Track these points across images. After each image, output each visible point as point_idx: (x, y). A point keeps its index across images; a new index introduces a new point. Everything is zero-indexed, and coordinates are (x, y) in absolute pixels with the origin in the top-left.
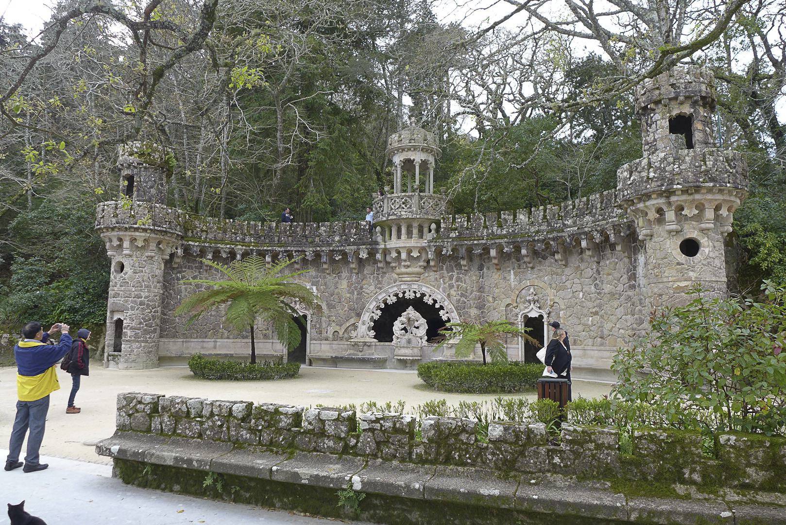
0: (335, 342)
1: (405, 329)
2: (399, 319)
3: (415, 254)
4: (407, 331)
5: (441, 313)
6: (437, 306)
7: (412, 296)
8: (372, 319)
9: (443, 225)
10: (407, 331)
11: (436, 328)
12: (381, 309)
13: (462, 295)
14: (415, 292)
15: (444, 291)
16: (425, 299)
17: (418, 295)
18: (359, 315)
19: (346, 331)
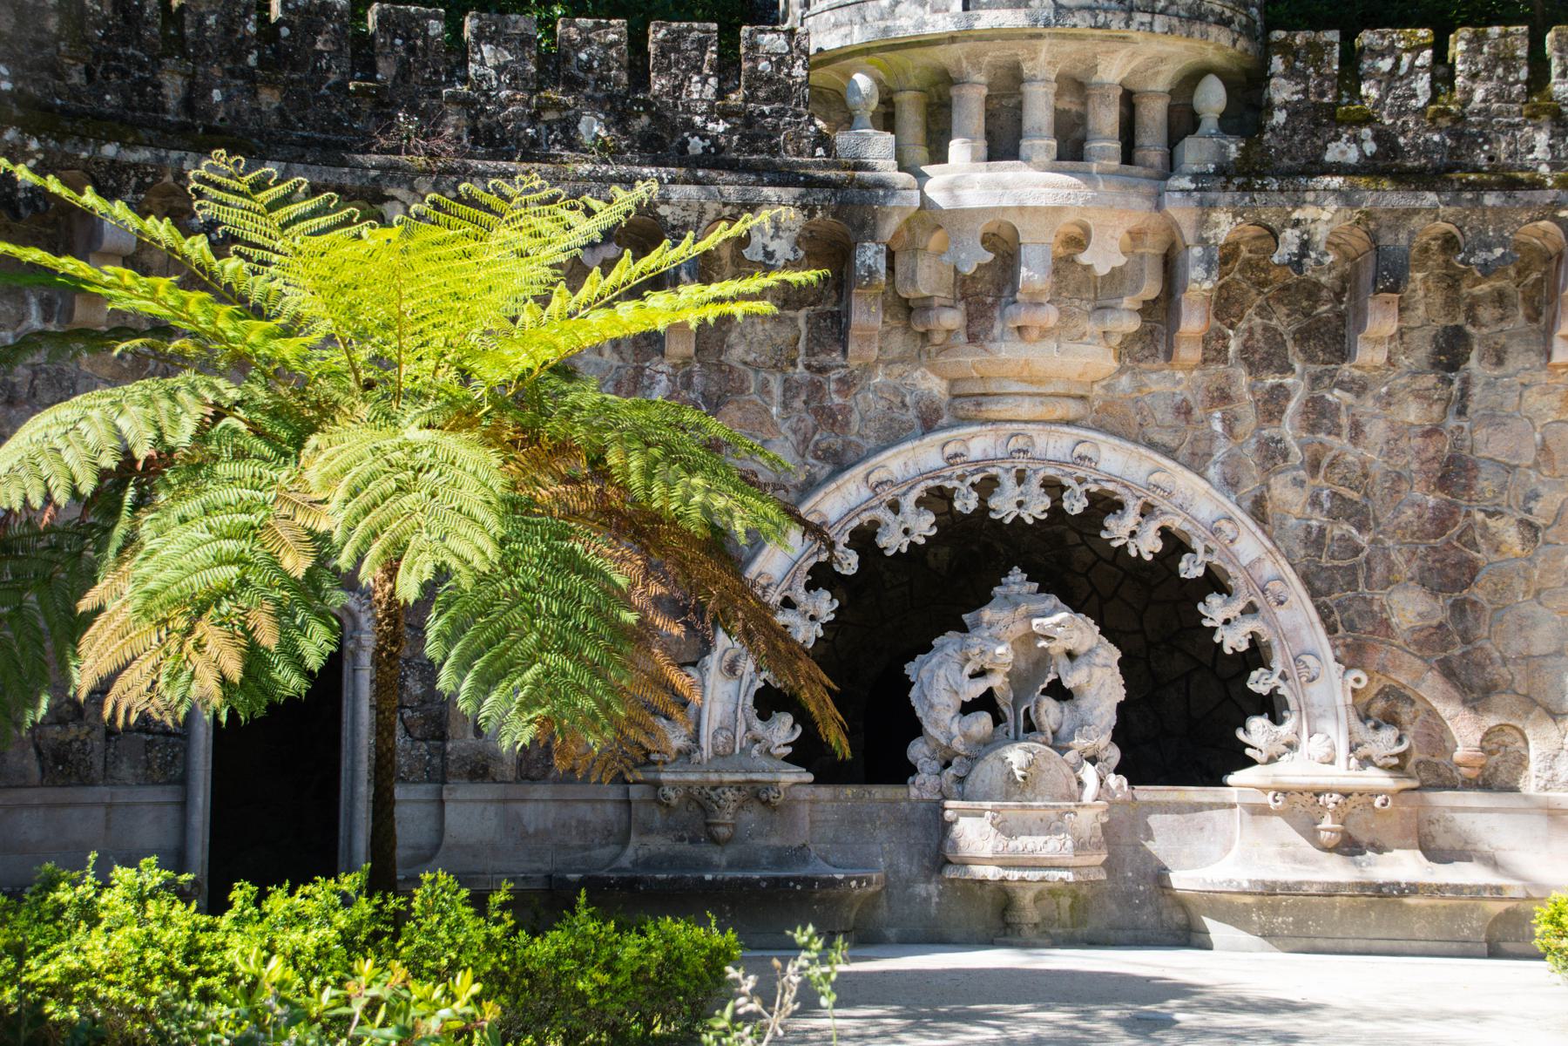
0: (541, 791)
1: (986, 702)
3: (1102, 257)
5: (1214, 610)
6: (1190, 569)
7: (1038, 507)
9: (1282, 91)
13: (1343, 509)
14: (1054, 488)
15: (1231, 484)
16: (1117, 529)
17: (1075, 505)
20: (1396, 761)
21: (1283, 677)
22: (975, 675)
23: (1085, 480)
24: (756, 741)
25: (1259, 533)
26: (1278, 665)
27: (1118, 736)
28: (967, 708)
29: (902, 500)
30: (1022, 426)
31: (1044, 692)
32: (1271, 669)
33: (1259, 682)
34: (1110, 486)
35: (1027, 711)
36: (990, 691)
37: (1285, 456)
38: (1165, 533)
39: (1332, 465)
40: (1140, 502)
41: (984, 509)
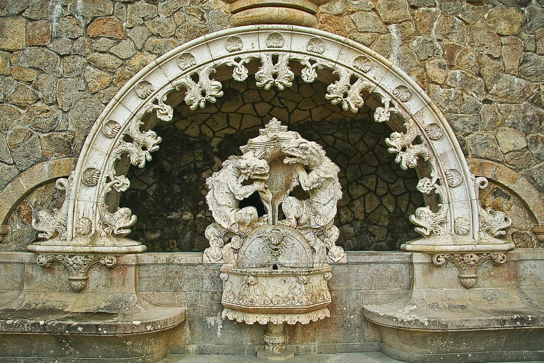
1: (255, 200)
2: (230, 165)
4: (262, 211)
8: (122, 163)
10: (262, 211)
11: (382, 199)
12: (160, 128)
14: (295, 65)
17: (309, 75)
18: (70, 149)
19: (15, 208)
20: (503, 233)
21: (438, 182)
22: (245, 183)
23: (315, 62)
24: (107, 226)
25: (423, 93)
26: (435, 175)
27: (338, 221)
28: (242, 204)
29: (200, 74)
30: (275, 26)
31: (291, 194)
32: (431, 178)
33: (424, 186)
34: (329, 65)
35: (280, 206)
36: (256, 194)
37: (434, 48)
38: (364, 93)
39: (460, 57)
40: (349, 75)
41: (251, 79)
